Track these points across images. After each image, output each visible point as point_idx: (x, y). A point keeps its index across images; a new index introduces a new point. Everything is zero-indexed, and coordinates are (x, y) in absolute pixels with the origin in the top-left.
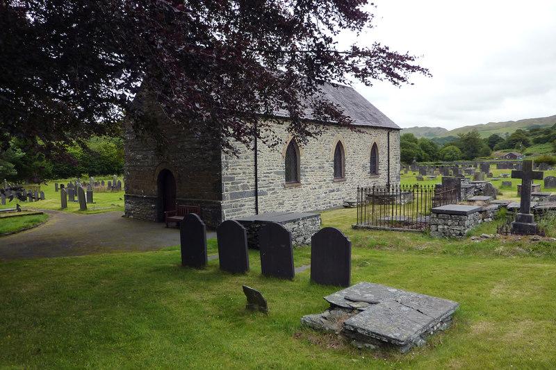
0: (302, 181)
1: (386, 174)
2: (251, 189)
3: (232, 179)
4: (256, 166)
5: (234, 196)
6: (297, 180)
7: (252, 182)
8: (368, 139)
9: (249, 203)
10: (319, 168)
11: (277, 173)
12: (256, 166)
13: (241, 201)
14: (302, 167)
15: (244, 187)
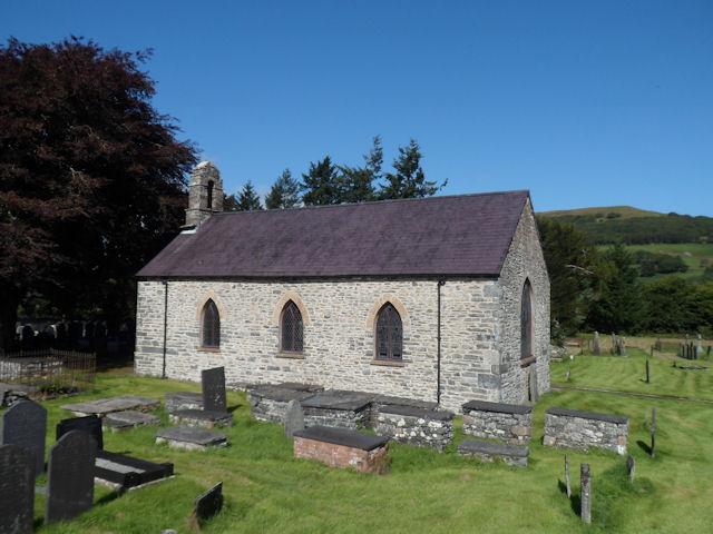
0: (222, 347)
1: (431, 363)
2: (161, 346)
3: (145, 334)
4: (166, 325)
5: (146, 350)
6: (217, 343)
7: (163, 339)
8: (374, 294)
9: (158, 360)
10: (252, 334)
11: (189, 334)
12: (166, 325)
13: (152, 355)
14: (223, 331)
15: (155, 343)
